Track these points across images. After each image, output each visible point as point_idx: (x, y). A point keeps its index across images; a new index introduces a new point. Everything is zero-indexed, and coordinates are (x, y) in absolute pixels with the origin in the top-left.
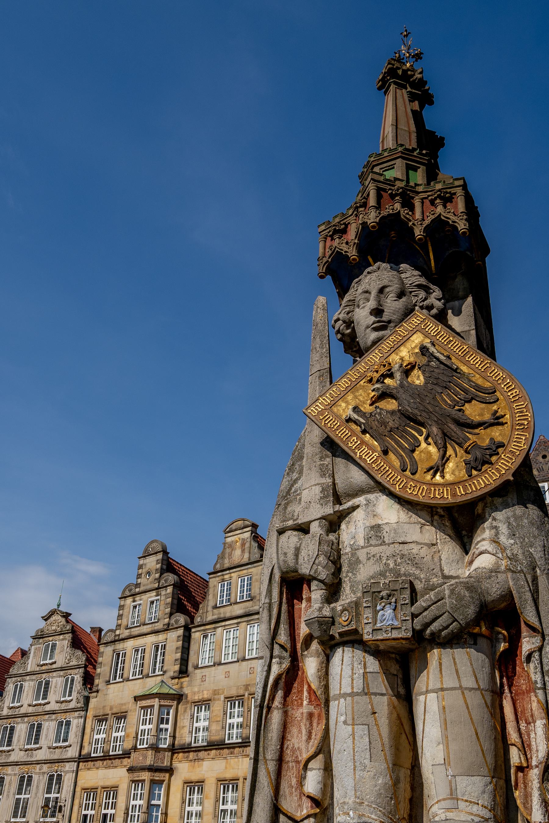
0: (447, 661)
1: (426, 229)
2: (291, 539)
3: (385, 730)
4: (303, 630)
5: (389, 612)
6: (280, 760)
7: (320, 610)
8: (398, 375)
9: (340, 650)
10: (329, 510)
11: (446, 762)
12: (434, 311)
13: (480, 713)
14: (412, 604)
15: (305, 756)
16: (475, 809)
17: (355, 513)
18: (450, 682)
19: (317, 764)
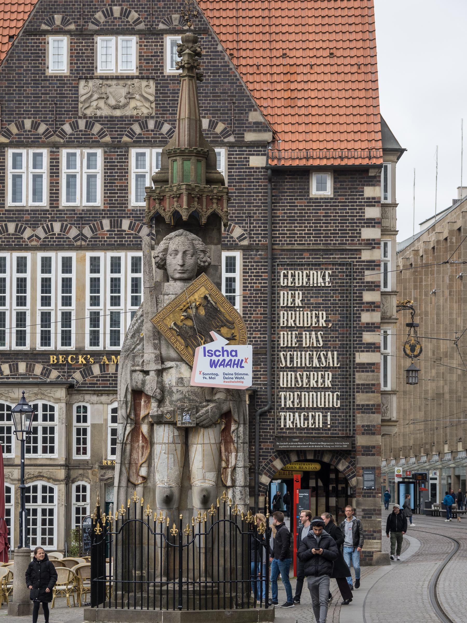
0: (206, 434)
1: (209, 218)
2: (140, 376)
3: (179, 456)
4: (143, 413)
5: (188, 417)
6: (130, 463)
7: (157, 411)
8: (194, 310)
9: (163, 426)
10: (160, 368)
11: (203, 468)
12: (207, 264)
13: (216, 452)
14: (197, 413)
15: (141, 462)
16: (211, 482)
17: (171, 370)
18: (206, 441)
19: (145, 465)
